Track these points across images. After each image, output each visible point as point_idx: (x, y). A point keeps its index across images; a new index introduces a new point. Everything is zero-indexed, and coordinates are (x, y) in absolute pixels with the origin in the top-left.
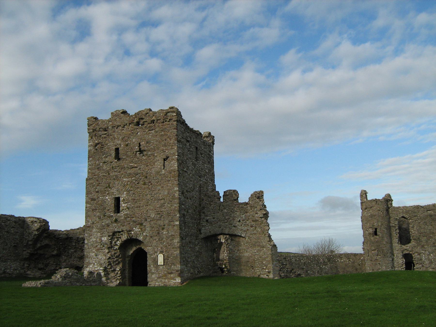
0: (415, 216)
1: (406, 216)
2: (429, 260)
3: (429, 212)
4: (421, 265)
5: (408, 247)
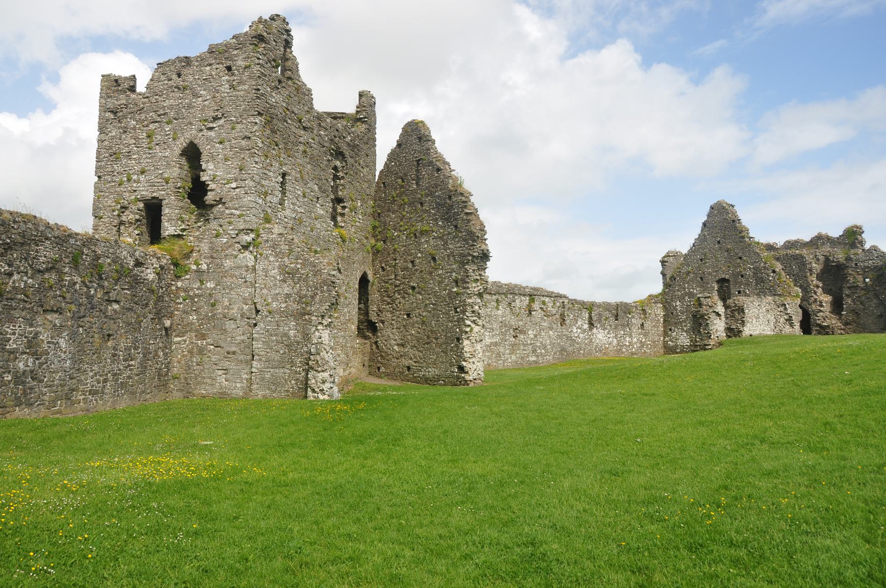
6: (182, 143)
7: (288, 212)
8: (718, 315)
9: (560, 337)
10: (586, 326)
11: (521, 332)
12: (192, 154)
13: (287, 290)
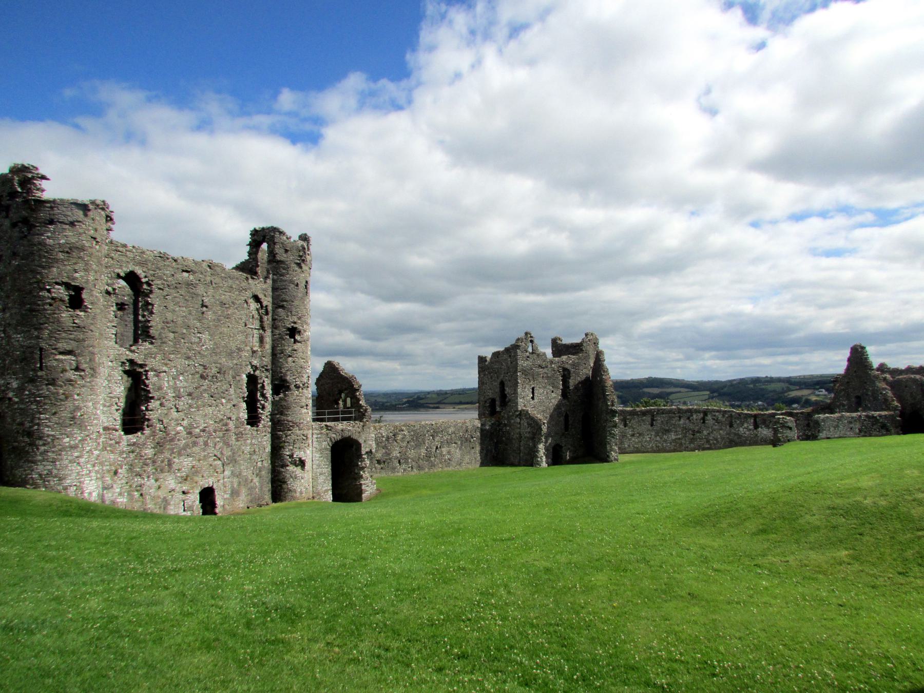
0: (160, 278)
1: (139, 271)
2: (175, 388)
3: (186, 274)
4: (158, 402)
5: (141, 352)
6: (499, 381)
7: (536, 400)
8: (790, 428)
9: (727, 434)
10: (751, 427)
11: (698, 432)
12: (502, 384)
13: (529, 430)
